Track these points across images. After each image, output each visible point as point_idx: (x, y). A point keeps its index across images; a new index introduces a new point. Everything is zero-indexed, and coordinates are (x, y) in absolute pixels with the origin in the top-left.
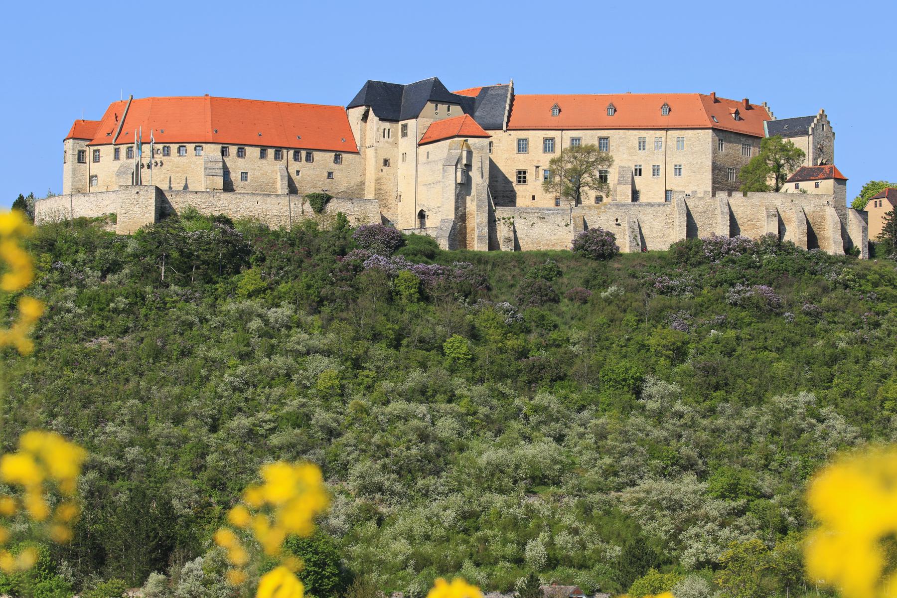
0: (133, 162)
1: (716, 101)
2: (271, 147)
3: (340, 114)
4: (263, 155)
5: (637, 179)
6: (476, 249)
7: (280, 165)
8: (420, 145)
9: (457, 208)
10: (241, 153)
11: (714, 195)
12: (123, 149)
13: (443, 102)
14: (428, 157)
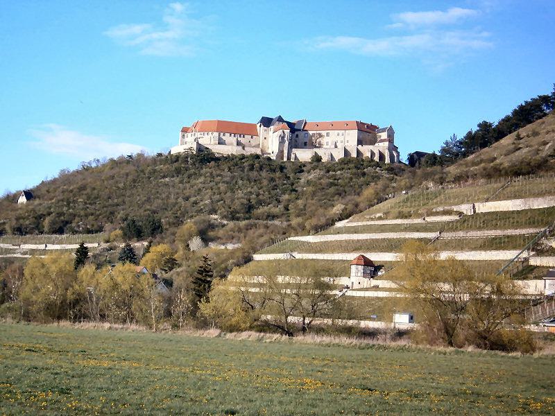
3: (255, 126)
10: (224, 135)
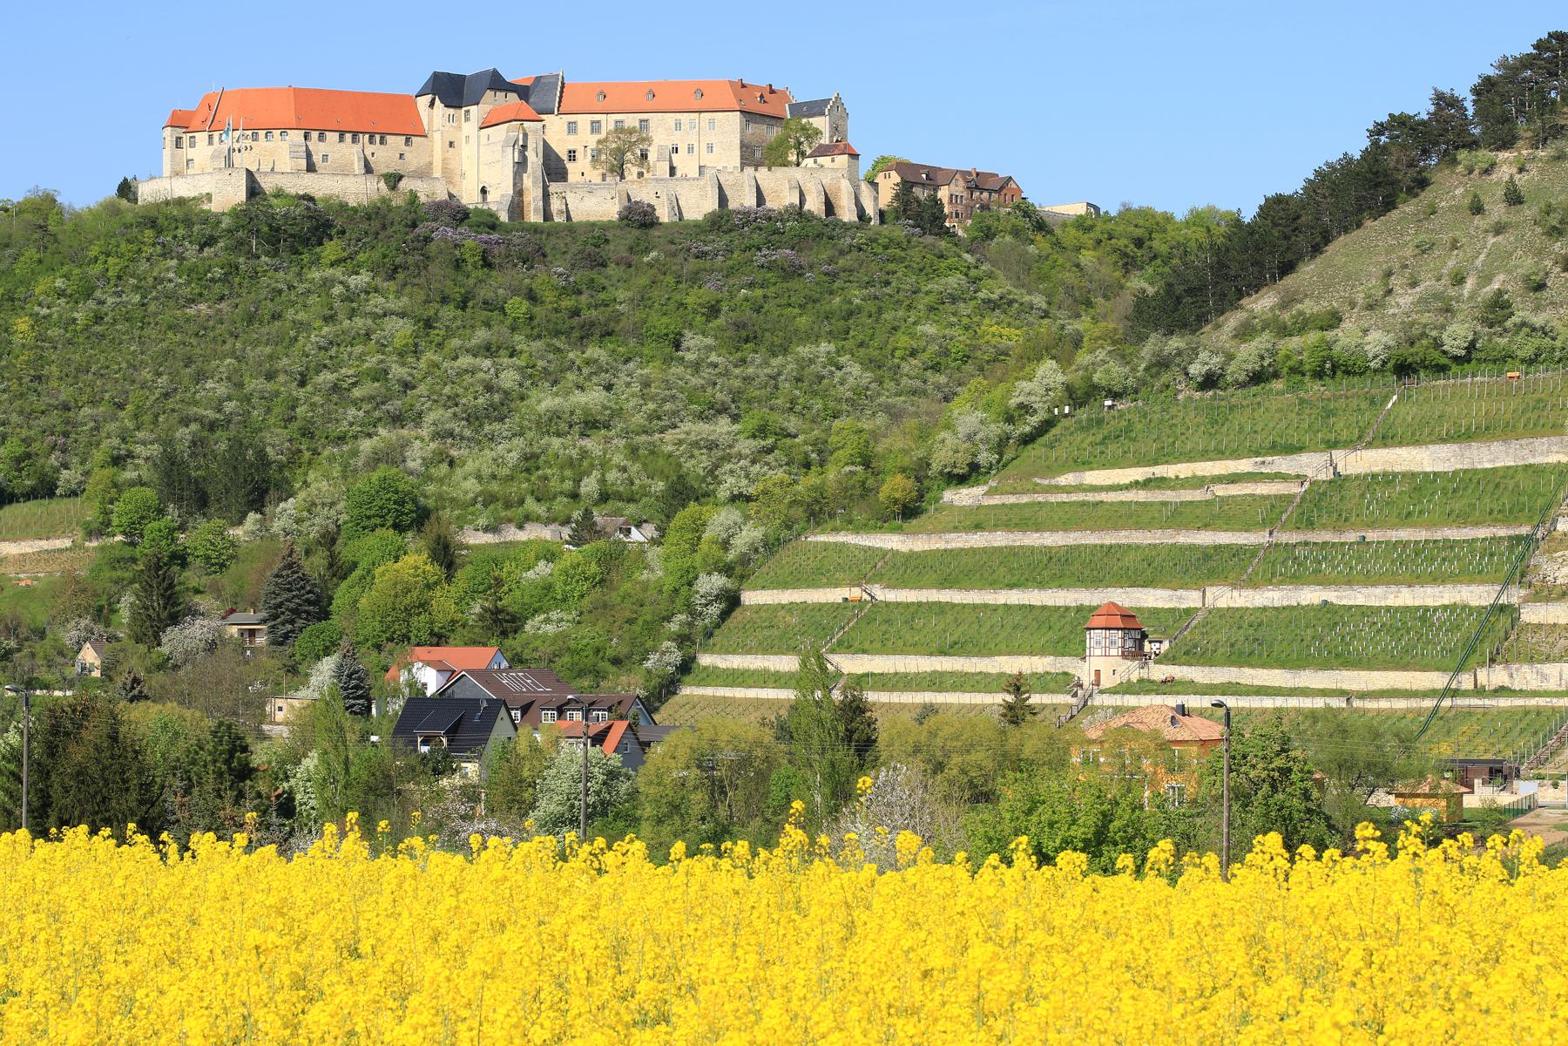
0: (225, 147)
1: (743, 86)
3: (407, 103)
4: (341, 139)
5: (674, 156)
7: (357, 148)
9: (515, 185)
10: (321, 138)
11: (742, 170)
13: (501, 90)
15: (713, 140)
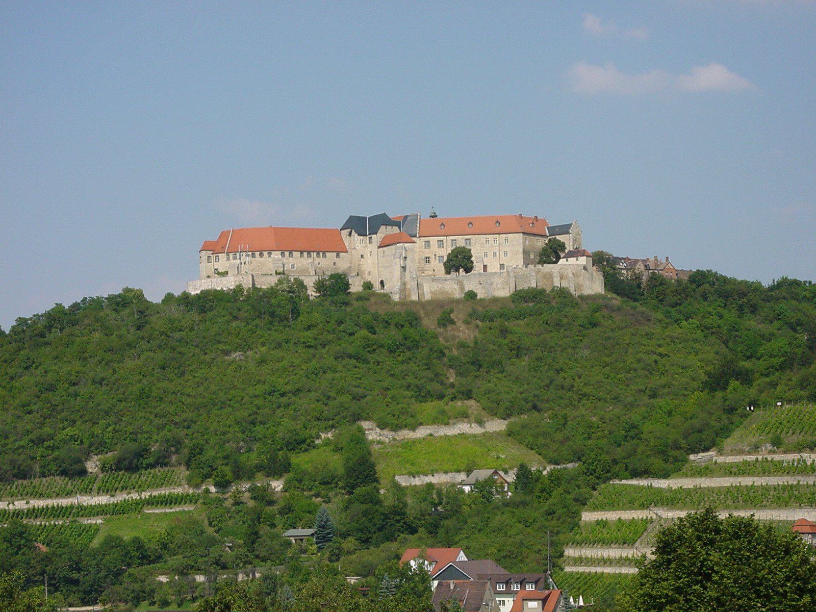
2: (305, 251)
6: (414, 299)
7: (310, 260)
8: (379, 247)
10: (291, 255)
12: (231, 255)
13: (389, 225)
14: (384, 253)
15: (507, 249)
